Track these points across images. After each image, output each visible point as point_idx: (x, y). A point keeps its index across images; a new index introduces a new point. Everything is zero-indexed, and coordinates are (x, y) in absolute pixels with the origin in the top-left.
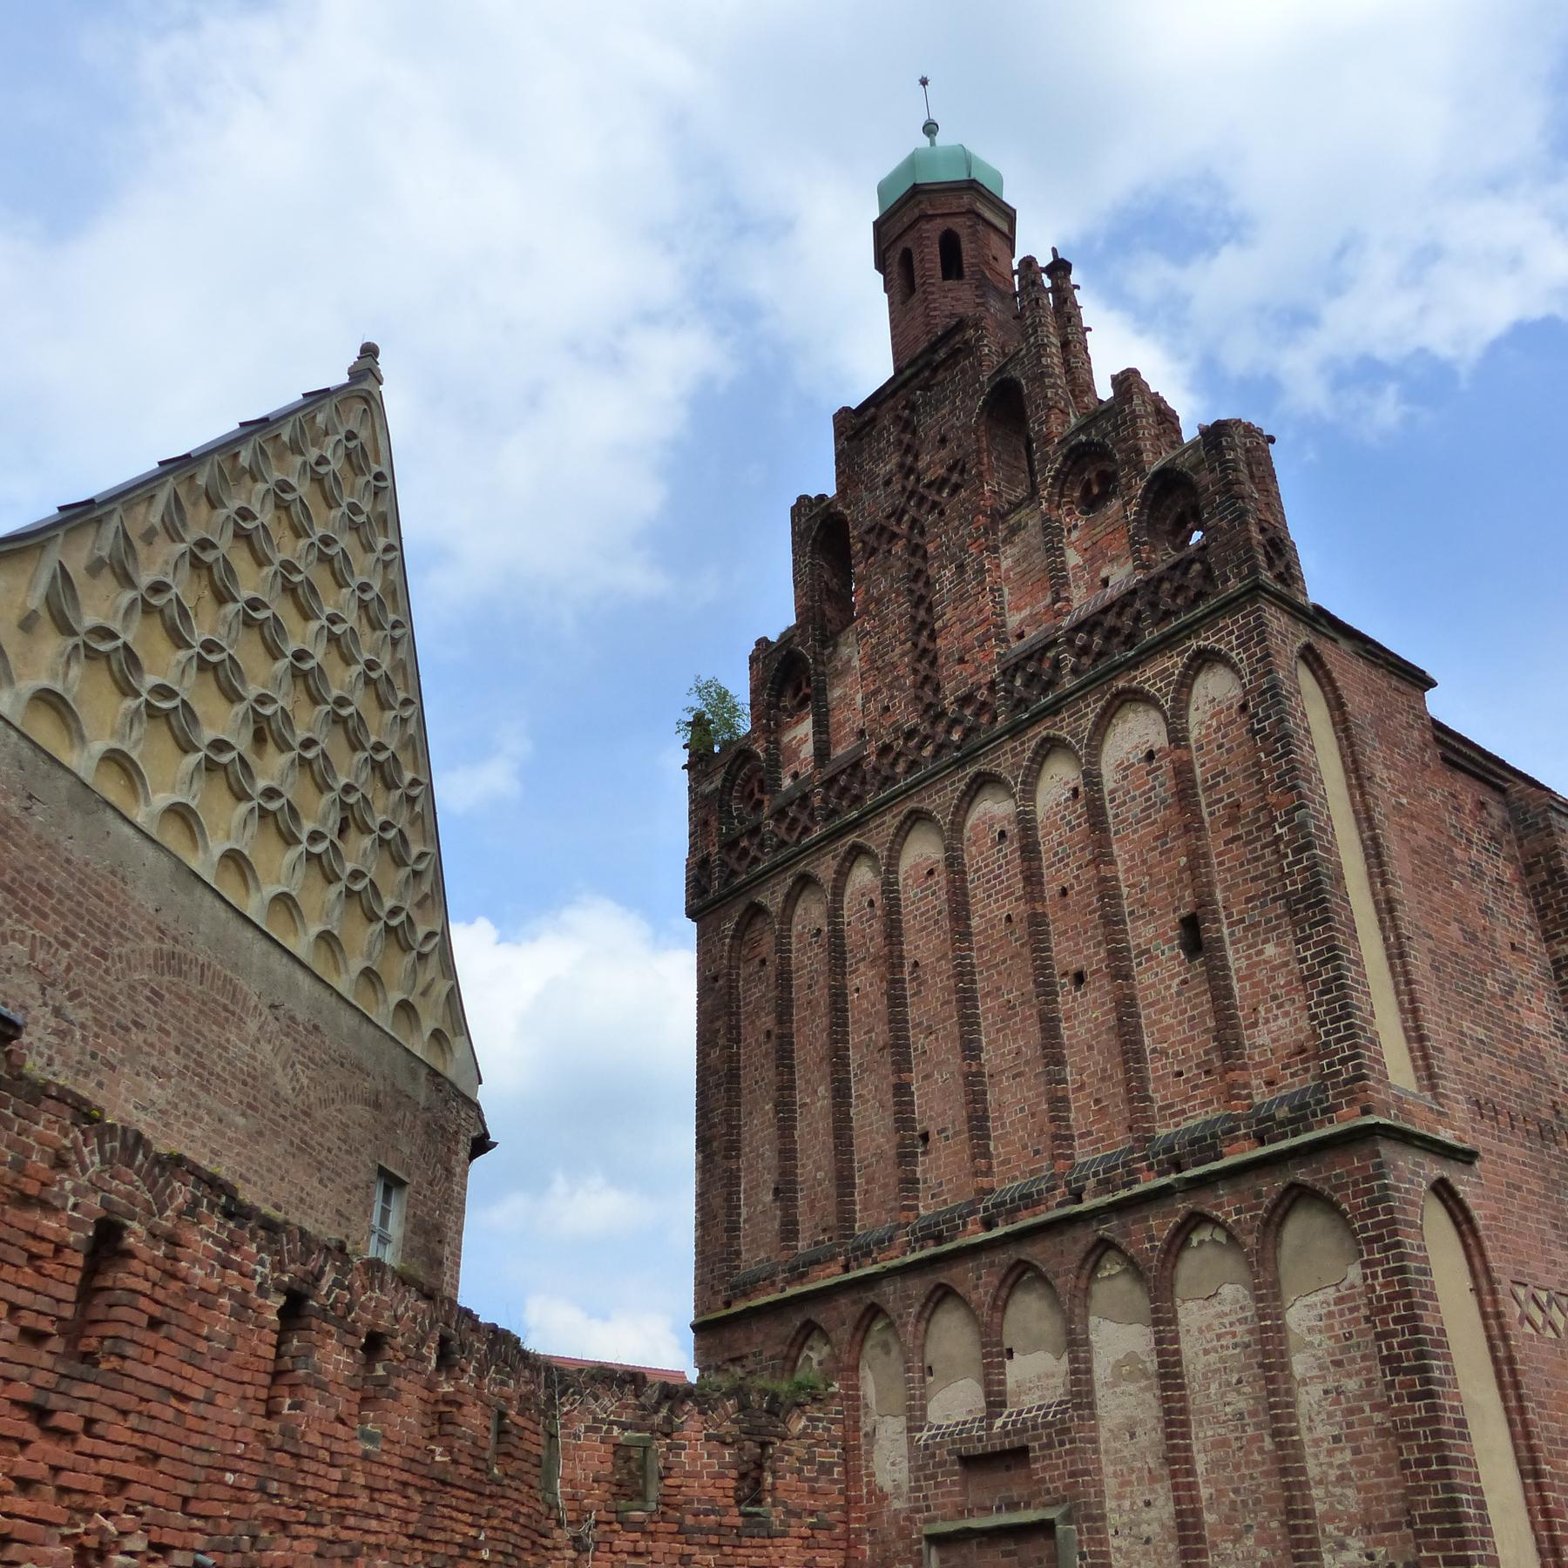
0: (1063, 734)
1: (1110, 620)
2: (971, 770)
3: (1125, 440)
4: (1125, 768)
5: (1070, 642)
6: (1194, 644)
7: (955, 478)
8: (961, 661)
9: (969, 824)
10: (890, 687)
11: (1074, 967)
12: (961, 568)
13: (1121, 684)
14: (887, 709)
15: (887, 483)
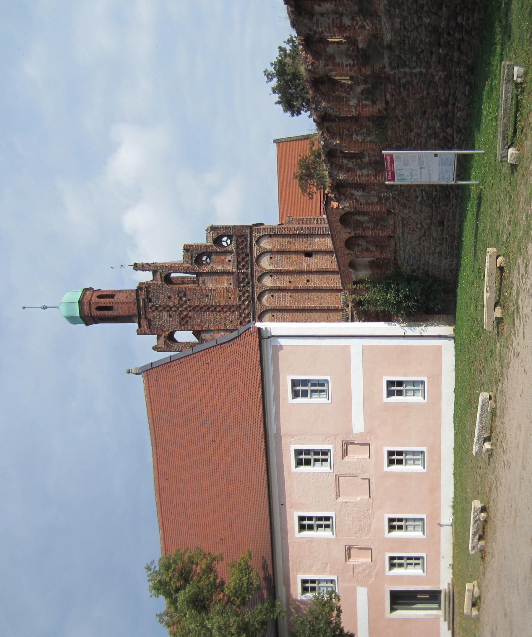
0: (258, 275)
1: (240, 259)
2: (256, 299)
3: (201, 248)
4: (271, 264)
5: (240, 269)
6: (254, 242)
7: (182, 295)
8: (230, 298)
9: (266, 304)
10: (226, 320)
11: (306, 282)
12: (207, 296)
13: (254, 260)
14: (231, 322)
15: (170, 316)
